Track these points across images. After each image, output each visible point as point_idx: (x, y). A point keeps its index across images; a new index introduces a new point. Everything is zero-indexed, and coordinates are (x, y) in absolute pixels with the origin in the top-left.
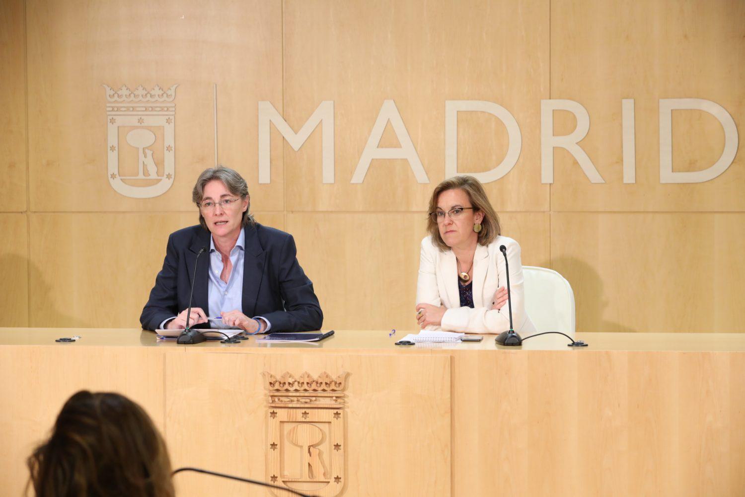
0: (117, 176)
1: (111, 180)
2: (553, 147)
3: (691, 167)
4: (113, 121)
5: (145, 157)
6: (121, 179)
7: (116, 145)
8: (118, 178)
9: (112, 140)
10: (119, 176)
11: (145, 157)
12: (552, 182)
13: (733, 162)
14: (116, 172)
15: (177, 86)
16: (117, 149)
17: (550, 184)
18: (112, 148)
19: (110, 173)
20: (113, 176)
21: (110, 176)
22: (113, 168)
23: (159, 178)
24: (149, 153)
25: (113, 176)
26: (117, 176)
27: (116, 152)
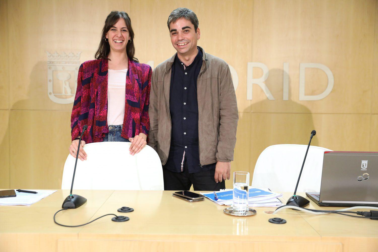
0: (52, 94)
1: (49, 95)
2: (253, 84)
3: (313, 93)
4: (50, 68)
5: (66, 85)
6: (54, 95)
7: (51, 79)
8: (53, 95)
9: (50, 77)
10: (53, 93)
11: (66, 85)
12: (251, 99)
13: (331, 92)
14: (52, 92)
15: (80, 54)
16: (52, 81)
17: (251, 100)
18: (50, 81)
19: (49, 92)
20: (50, 94)
21: (49, 93)
22: (50, 90)
23: (72, 95)
24: (67, 83)
25: (50, 94)
26: (52, 94)
27: (52, 83)
